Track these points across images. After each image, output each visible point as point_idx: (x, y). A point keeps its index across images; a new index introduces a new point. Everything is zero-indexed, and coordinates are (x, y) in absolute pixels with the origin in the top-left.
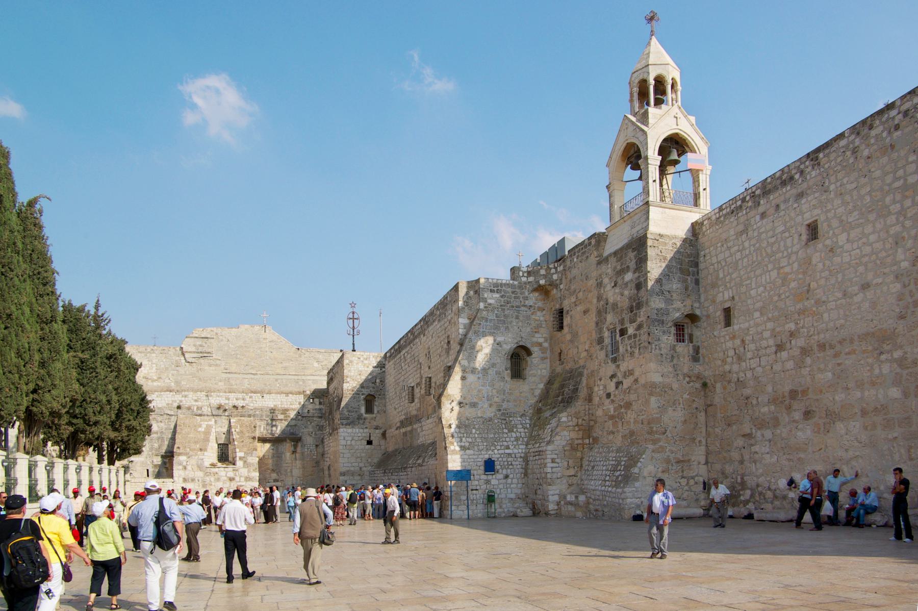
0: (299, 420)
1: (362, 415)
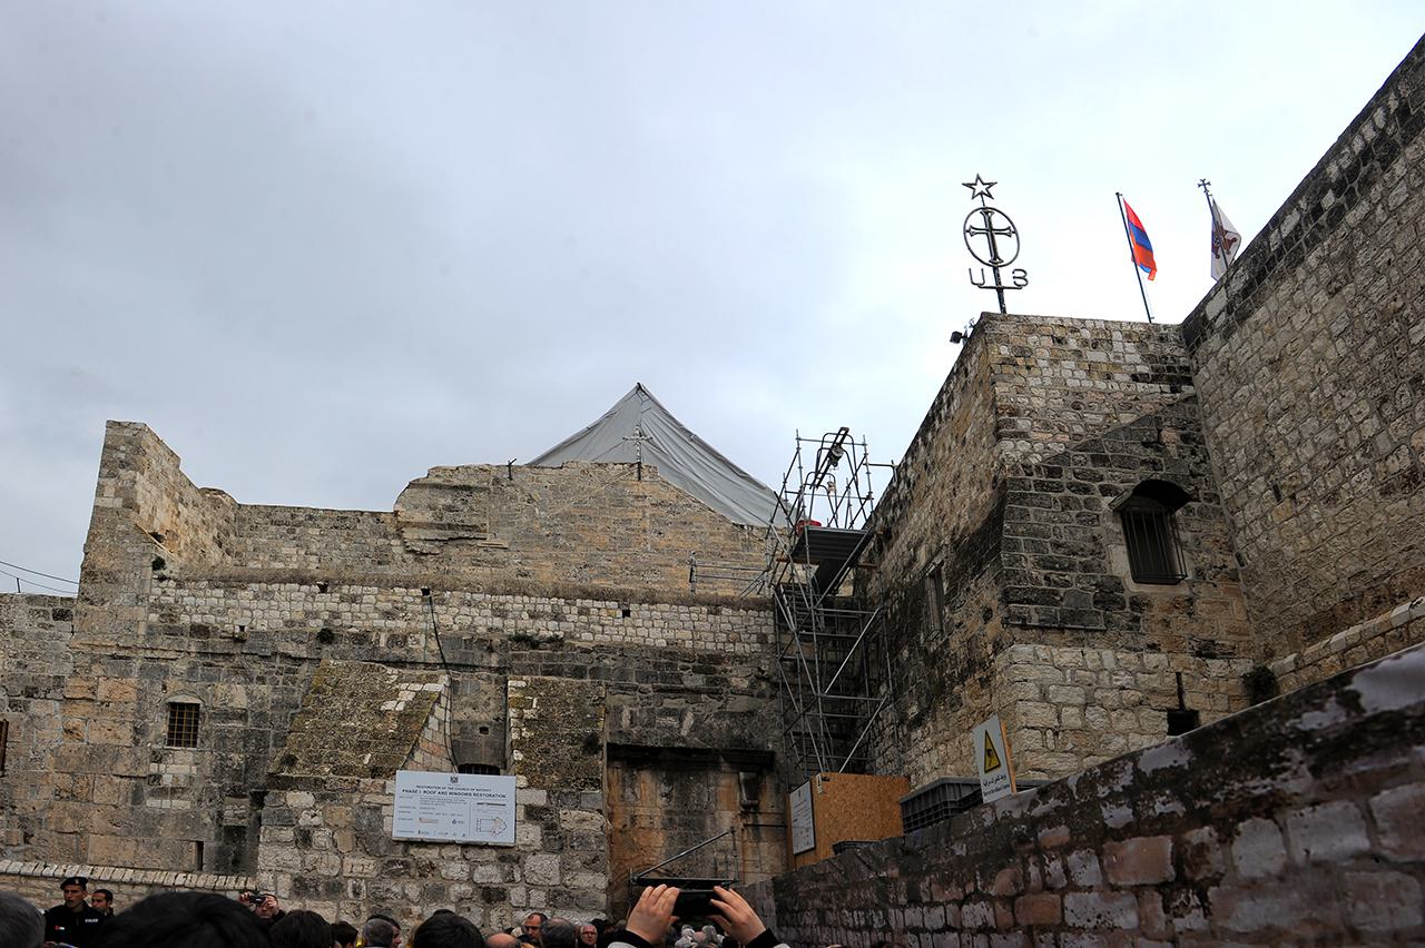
0: (761, 695)
1: (1118, 585)
